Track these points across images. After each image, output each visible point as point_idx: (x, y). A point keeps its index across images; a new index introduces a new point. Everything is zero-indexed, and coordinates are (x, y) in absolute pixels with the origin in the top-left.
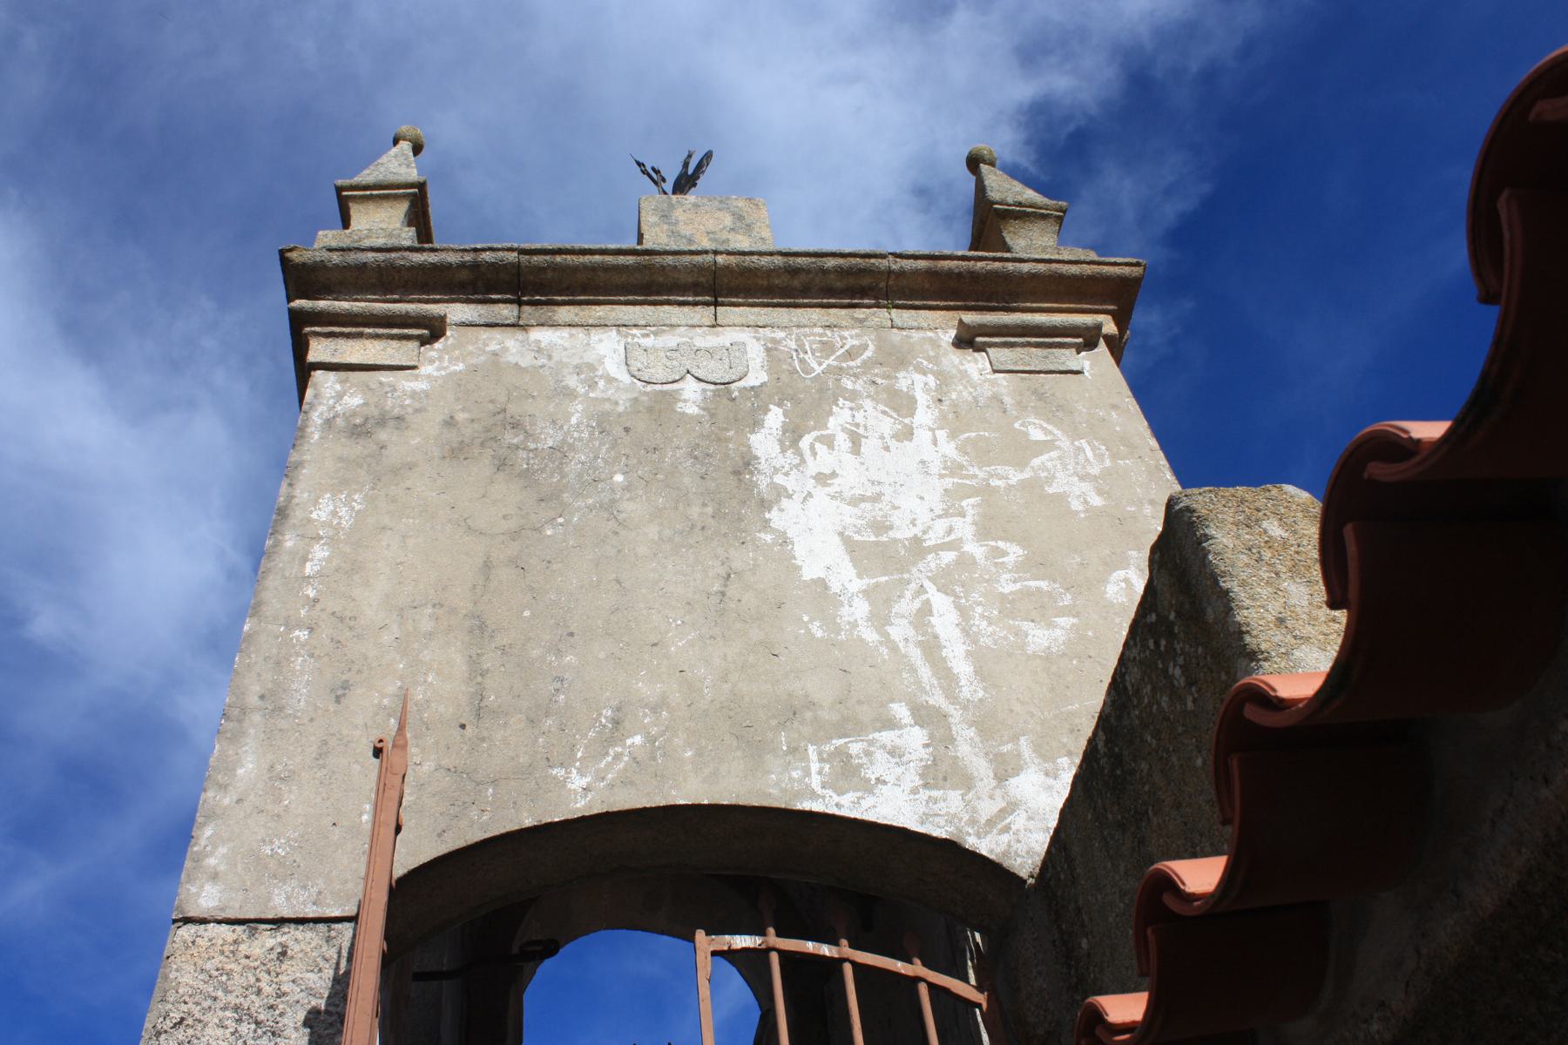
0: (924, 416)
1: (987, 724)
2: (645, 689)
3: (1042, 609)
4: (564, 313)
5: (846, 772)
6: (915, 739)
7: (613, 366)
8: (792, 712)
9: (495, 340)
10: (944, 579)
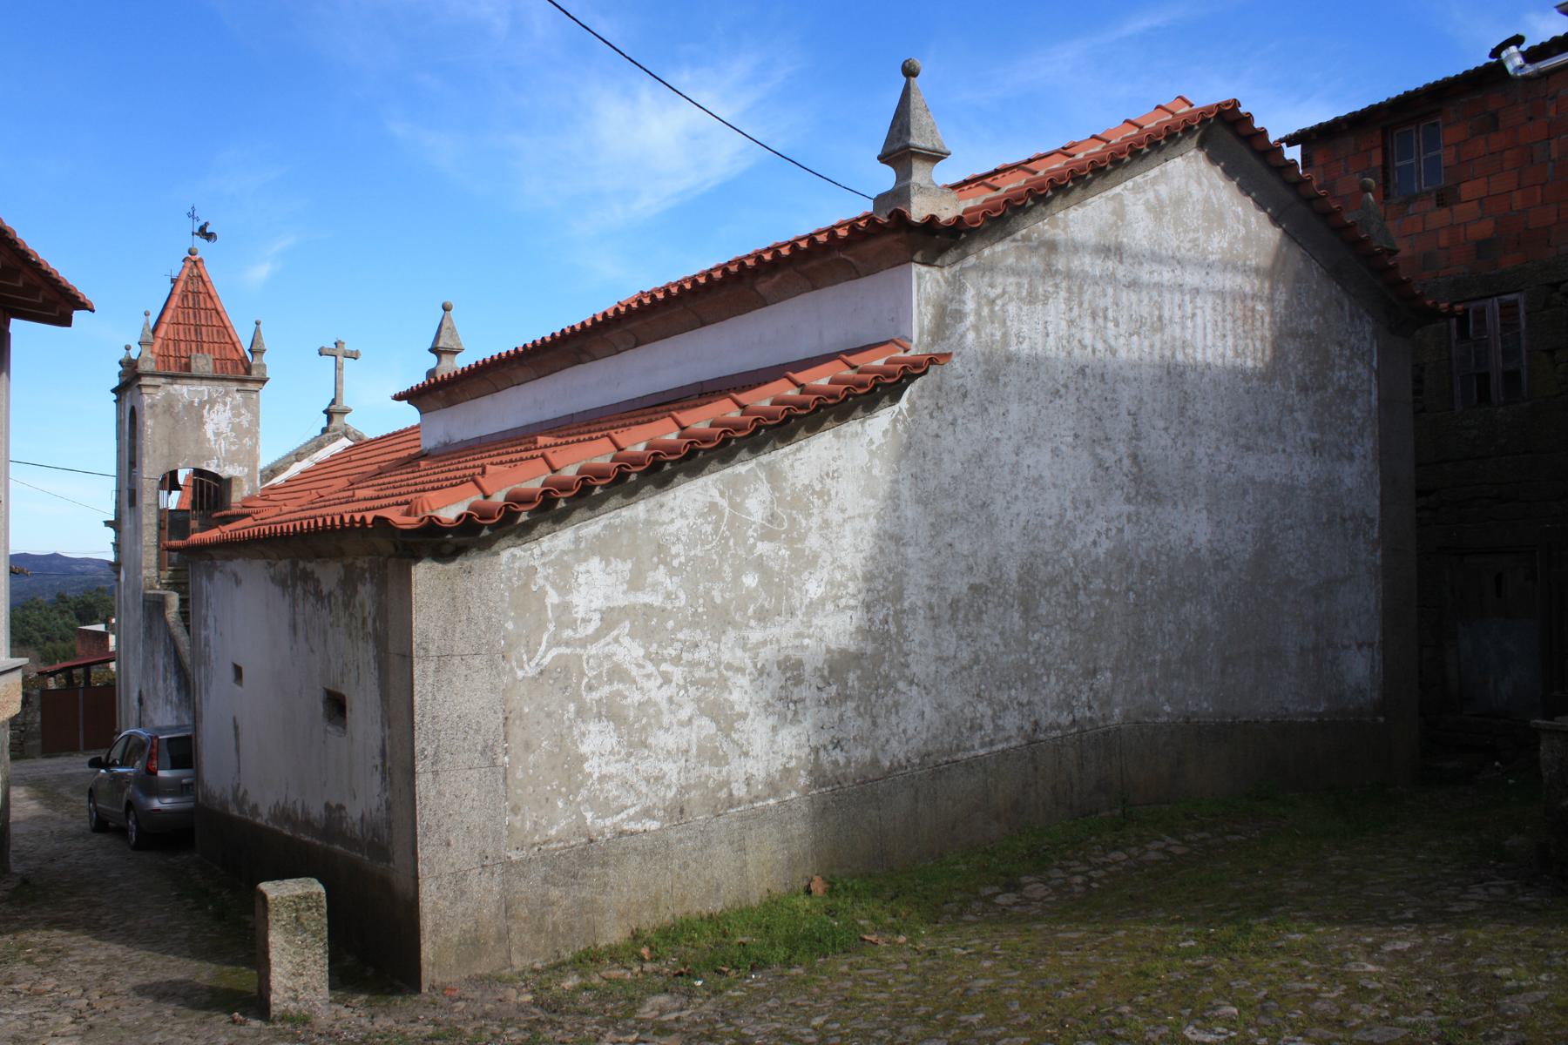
0: (228, 407)
1: (224, 460)
2: (188, 453)
3: (233, 443)
4: (179, 381)
5: (208, 465)
6: (216, 461)
7: (185, 394)
8: (203, 457)
9: (170, 388)
10: (224, 439)
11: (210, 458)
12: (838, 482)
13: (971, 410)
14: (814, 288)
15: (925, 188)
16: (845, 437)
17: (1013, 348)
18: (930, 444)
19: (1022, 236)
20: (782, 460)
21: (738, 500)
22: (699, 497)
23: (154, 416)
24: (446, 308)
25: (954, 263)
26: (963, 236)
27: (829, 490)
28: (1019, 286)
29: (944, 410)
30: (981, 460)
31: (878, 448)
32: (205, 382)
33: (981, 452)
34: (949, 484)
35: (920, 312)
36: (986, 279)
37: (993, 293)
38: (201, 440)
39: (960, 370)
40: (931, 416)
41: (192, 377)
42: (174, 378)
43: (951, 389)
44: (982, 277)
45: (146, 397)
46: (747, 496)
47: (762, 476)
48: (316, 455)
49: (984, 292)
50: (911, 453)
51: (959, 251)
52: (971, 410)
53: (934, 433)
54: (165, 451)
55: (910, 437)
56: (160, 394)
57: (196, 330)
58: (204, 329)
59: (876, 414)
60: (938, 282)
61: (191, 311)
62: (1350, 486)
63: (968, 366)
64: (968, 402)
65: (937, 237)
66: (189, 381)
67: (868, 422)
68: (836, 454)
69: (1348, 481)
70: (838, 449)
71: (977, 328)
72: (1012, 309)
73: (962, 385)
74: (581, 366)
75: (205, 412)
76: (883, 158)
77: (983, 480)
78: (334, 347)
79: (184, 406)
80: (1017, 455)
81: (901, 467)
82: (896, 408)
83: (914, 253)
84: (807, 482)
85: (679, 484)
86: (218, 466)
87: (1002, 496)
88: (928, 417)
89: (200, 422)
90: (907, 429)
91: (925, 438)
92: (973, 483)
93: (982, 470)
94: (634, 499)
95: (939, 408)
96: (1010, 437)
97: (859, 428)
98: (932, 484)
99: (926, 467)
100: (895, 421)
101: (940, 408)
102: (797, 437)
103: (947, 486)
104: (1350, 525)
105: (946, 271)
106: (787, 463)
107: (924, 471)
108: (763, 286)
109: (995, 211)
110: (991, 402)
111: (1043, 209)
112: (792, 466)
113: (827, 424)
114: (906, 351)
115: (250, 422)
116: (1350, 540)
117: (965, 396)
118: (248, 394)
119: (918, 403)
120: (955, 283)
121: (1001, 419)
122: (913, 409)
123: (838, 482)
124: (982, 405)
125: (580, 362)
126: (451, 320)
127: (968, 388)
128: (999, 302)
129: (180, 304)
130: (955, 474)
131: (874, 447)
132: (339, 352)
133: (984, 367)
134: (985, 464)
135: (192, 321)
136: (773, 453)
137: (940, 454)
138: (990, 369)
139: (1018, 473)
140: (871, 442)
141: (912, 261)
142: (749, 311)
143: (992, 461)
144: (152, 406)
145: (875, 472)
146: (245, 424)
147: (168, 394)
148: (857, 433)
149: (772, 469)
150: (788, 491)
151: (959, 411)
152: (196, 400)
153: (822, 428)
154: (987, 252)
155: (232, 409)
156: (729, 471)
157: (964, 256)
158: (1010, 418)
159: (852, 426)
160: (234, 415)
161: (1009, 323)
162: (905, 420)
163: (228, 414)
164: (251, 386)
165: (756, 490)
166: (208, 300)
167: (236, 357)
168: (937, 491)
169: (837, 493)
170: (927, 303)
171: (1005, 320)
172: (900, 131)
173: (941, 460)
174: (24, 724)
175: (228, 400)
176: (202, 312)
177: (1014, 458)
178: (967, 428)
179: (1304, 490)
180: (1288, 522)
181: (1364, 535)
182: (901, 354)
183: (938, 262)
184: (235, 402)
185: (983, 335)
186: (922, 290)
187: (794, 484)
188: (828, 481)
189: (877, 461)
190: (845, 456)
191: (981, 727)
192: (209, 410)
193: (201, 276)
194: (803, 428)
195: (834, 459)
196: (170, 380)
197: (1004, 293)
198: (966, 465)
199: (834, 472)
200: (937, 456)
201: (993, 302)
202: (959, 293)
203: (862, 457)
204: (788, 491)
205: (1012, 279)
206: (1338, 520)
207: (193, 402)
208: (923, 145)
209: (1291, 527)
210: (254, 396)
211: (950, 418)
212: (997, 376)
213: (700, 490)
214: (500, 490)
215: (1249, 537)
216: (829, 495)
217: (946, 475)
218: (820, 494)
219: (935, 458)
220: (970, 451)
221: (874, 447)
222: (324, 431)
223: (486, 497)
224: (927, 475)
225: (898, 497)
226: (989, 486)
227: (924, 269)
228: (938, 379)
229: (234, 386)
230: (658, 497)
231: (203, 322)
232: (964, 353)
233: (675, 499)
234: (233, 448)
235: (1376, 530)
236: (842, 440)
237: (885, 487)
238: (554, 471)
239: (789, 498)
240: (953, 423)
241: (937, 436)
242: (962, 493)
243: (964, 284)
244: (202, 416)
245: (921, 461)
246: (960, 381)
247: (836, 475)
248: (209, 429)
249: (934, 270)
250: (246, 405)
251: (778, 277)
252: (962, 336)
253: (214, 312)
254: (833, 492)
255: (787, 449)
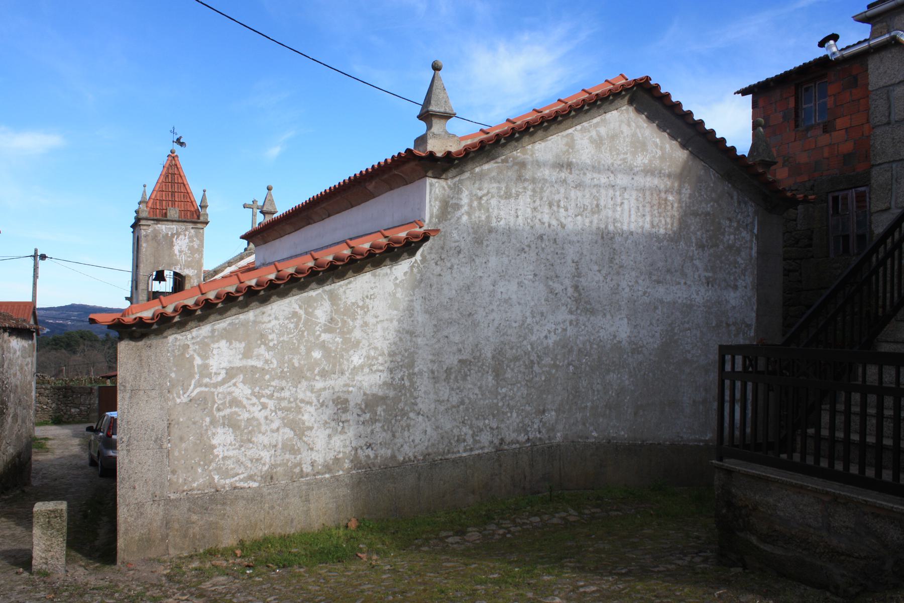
1: (184, 266)
3: (189, 257)
4: (161, 223)
6: (179, 266)
7: (164, 230)
8: (173, 264)
11: (177, 265)
12: (374, 301)
13: (463, 260)
14: (391, 189)
15: (437, 135)
16: (379, 276)
17: (494, 224)
18: (435, 280)
19: (502, 160)
20: (338, 289)
21: (311, 310)
22: (286, 309)
23: (147, 241)
24: (269, 189)
25: (455, 177)
26: (456, 162)
27: (368, 305)
28: (499, 189)
29: (445, 260)
30: (469, 289)
31: (400, 282)
32: (174, 223)
33: (469, 284)
34: (447, 302)
35: (431, 205)
36: (477, 185)
37: (480, 193)
38: (171, 255)
39: (457, 238)
40: (436, 264)
41: (168, 221)
42: (158, 221)
43: (451, 248)
44: (473, 184)
45: (143, 231)
46: (315, 308)
47: (326, 297)
48: (239, 263)
49: (474, 193)
50: (422, 285)
51: (457, 170)
52: (463, 260)
53: (438, 273)
54: (152, 261)
55: (422, 276)
56: (150, 230)
57: (172, 195)
58: (176, 194)
59: (399, 263)
60: (444, 188)
61: (170, 184)
62: (734, 305)
63: (462, 236)
64: (461, 256)
65: (439, 163)
66: (166, 223)
67: (394, 267)
68: (373, 285)
69: (733, 302)
70: (375, 283)
71: (469, 214)
72: (494, 202)
73: (458, 246)
74: (310, 226)
75: (174, 240)
76: (420, 117)
77: (470, 300)
78: (252, 203)
79: (163, 236)
80: (494, 286)
81: (415, 293)
82: (413, 259)
83: (427, 172)
84: (353, 301)
85: (274, 302)
86: (180, 269)
87: (482, 309)
88: (434, 264)
89: (171, 245)
90: (420, 272)
91: (431, 276)
92: (463, 302)
93: (470, 294)
94: (246, 309)
95: (441, 259)
96: (489, 276)
97: (389, 271)
98: (436, 302)
99: (432, 293)
100: (412, 267)
101: (442, 259)
102: (347, 276)
103: (445, 303)
104: (733, 328)
105: (449, 182)
106: (341, 290)
107: (431, 295)
108: (371, 187)
109: (473, 148)
110: (477, 256)
111: (516, 144)
112: (345, 292)
113: (367, 269)
114: (420, 227)
115: (198, 245)
116: (733, 337)
117: (459, 252)
118: (197, 230)
119: (428, 257)
120: (455, 188)
121: (484, 265)
122: (424, 259)
123: (374, 301)
124: (471, 257)
125: (309, 224)
126: (271, 195)
127: (462, 248)
128: (485, 198)
129: (164, 181)
130: (451, 297)
131: (398, 282)
132: (255, 206)
133: (474, 236)
134: (471, 291)
135: (170, 190)
136: (333, 285)
137: (441, 286)
138: (477, 236)
139: (494, 296)
140: (396, 278)
141: (427, 176)
142: (368, 200)
143: (477, 289)
144: (146, 236)
145: (399, 295)
146: (196, 246)
147: (155, 229)
148: (387, 274)
149: (332, 294)
150: (342, 306)
151: (454, 261)
152: (170, 233)
153: (364, 271)
154: (477, 170)
155: (189, 238)
156: (305, 294)
157: (462, 172)
158: (490, 265)
159: (384, 270)
160: (190, 242)
161: (491, 210)
162: (419, 266)
163: (187, 240)
164: (199, 226)
165: (322, 305)
166: (180, 178)
167: (193, 209)
168: (439, 306)
169: (373, 307)
170: (436, 200)
171: (488, 209)
172: (427, 102)
173: (442, 289)
174: (90, 404)
175: (187, 233)
176: (176, 185)
177: (492, 288)
178: (460, 270)
179: (699, 307)
180: (687, 326)
181: (743, 335)
182: (418, 229)
183: (444, 176)
184: (190, 234)
185: (473, 217)
186: (433, 192)
187: (345, 302)
188: (368, 300)
189: (399, 290)
190: (379, 287)
191: (464, 441)
192: (177, 238)
193: (176, 165)
194: (351, 271)
195: (372, 288)
196: (156, 222)
197: (488, 193)
198: (458, 292)
199: (371, 295)
200: (439, 286)
201: (481, 198)
202: (458, 194)
203: (390, 287)
204: (342, 306)
205: (495, 185)
206: (724, 325)
207: (168, 234)
208: (438, 110)
209: (689, 329)
210: (201, 231)
211: (449, 265)
212: (482, 241)
213: (287, 305)
214: (172, 303)
215: (658, 335)
216: (368, 308)
217: (445, 298)
218: (362, 308)
219: (438, 288)
220: (461, 284)
221: (398, 282)
222: (246, 250)
223: (164, 307)
224: (432, 297)
225: (413, 310)
226: (474, 304)
227: (434, 180)
228: (442, 243)
229: (190, 226)
230: (261, 308)
231: (176, 190)
232: (460, 228)
233: (272, 309)
234: (189, 259)
235: (753, 331)
236: (377, 277)
237: (404, 304)
238: (203, 294)
239: (342, 310)
240: (451, 268)
241: (440, 275)
242: (456, 308)
243: (461, 188)
244: (173, 242)
245: (428, 289)
246: (457, 244)
247: (372, 297)
248: (176, 249)
249: (442, 182)
250: (197, 236)
251: (374, 183)
252: (459, 218)
253: (182, 185)
254: (370, 307)
255: (342, 283)
